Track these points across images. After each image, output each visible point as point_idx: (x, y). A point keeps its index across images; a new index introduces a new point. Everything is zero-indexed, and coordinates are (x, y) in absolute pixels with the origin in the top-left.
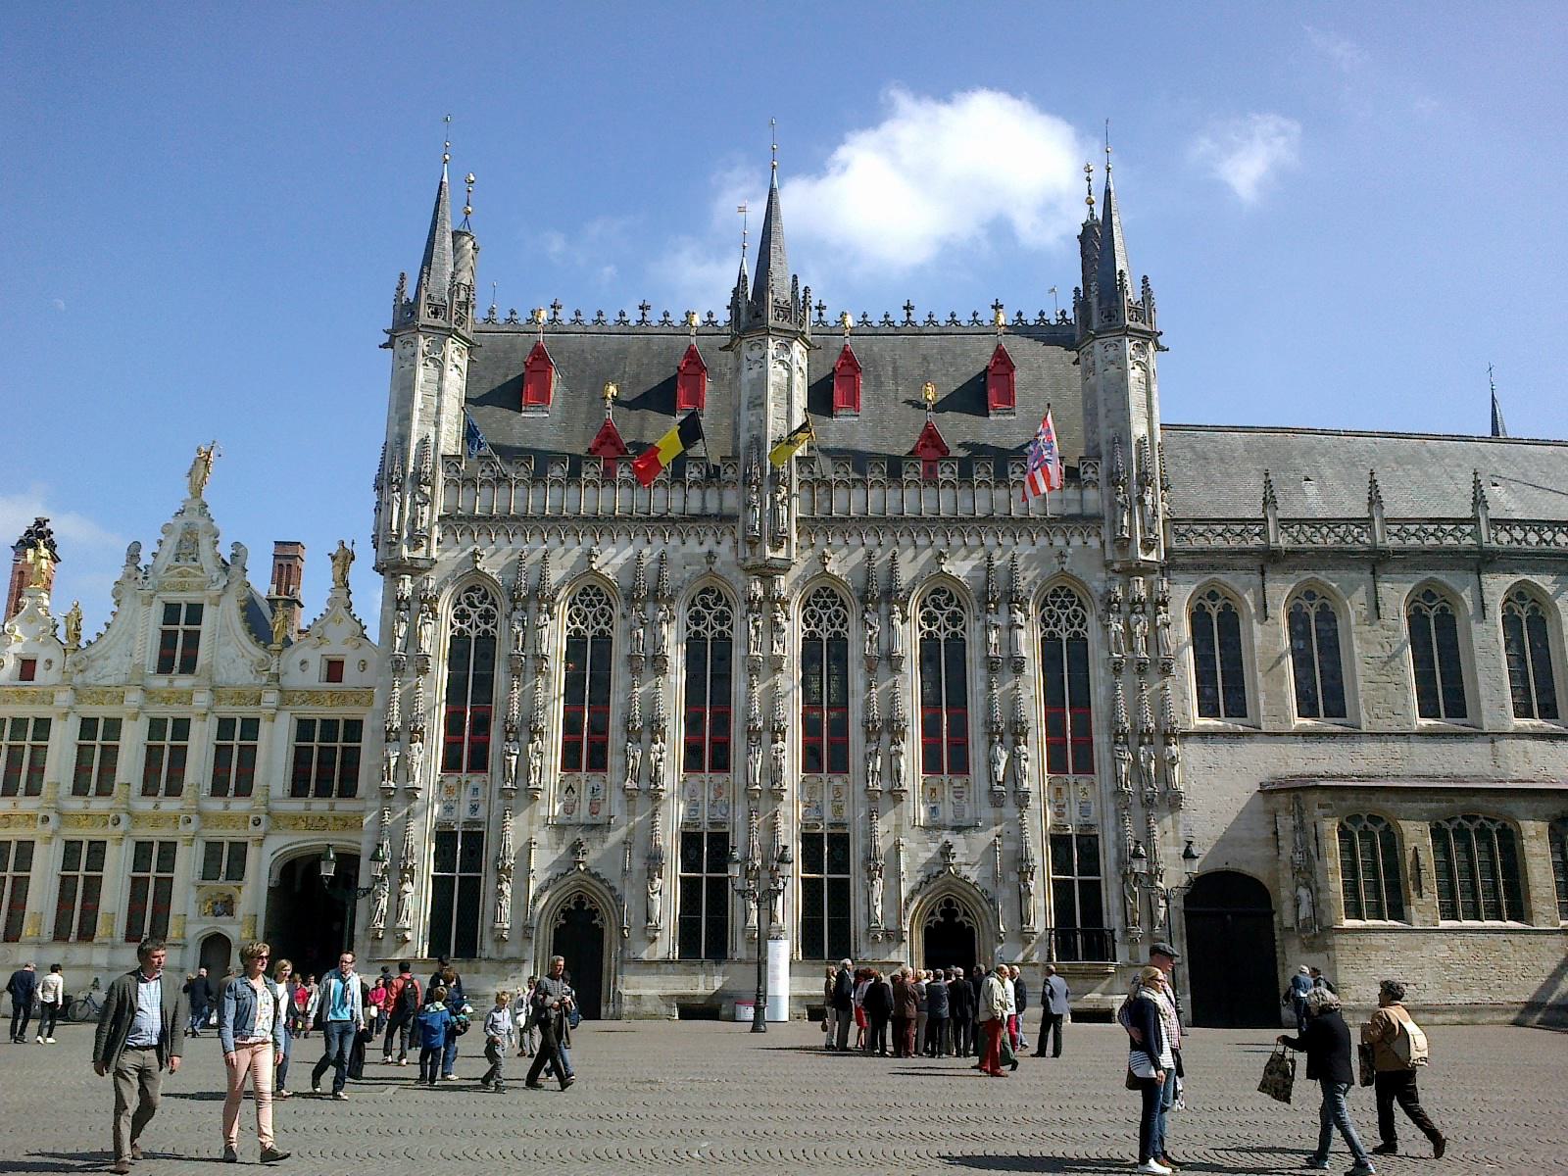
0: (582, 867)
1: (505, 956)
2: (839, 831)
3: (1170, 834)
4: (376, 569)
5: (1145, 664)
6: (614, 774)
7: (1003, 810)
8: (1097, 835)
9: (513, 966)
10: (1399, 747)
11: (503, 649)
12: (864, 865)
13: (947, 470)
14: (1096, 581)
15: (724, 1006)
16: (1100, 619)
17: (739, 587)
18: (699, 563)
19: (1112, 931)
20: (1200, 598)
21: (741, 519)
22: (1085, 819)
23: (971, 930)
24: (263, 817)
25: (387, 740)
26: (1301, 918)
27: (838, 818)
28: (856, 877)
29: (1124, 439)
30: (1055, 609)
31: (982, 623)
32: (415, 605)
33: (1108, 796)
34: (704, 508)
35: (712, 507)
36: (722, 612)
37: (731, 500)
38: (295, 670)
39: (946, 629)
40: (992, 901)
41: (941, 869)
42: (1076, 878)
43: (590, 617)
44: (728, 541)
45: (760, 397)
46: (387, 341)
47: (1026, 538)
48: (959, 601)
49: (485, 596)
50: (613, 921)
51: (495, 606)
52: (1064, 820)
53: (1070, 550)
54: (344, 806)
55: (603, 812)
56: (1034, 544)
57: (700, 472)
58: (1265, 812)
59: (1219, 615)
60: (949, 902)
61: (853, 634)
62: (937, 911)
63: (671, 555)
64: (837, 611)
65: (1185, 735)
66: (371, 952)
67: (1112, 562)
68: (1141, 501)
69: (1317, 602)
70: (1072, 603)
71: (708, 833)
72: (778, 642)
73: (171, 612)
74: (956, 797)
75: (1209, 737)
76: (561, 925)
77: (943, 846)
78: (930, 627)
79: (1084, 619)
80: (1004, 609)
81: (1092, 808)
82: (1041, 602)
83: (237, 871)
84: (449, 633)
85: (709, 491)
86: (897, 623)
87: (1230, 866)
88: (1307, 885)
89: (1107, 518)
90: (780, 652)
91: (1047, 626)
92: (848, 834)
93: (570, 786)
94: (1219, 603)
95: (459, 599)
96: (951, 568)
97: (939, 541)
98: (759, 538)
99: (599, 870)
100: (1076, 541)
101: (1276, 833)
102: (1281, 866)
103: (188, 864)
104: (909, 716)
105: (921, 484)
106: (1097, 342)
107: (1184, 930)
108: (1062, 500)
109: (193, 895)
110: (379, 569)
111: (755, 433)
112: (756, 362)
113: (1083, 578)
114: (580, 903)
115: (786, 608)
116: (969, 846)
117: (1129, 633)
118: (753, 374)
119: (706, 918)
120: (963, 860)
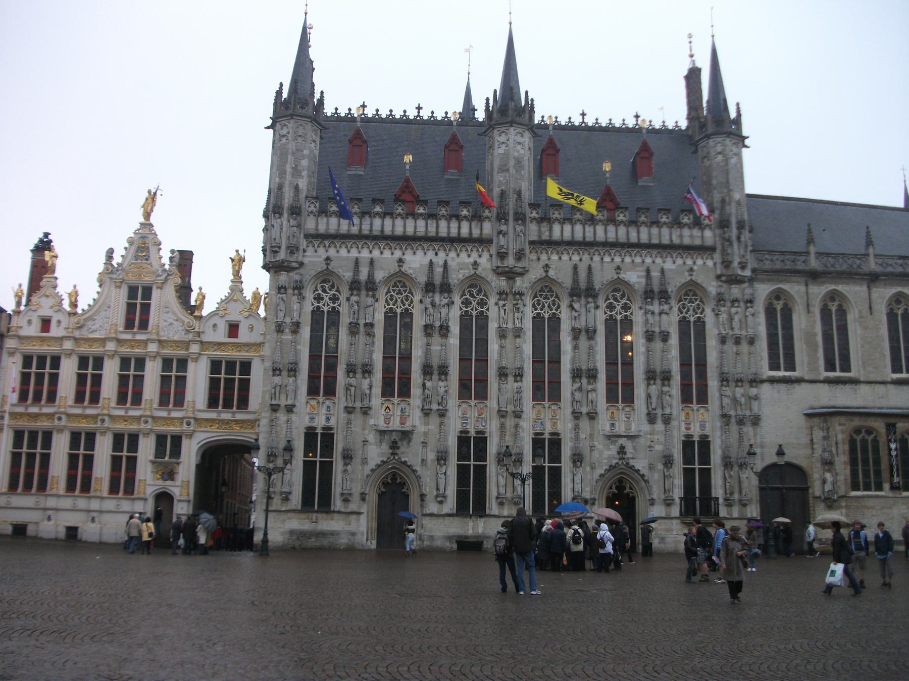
0: (397, 458)
1: (349, 510)
4: (264, 267)
7: (655, 426)
9: (354, 517)
10: (880, 389)
11: (345, 319)
13: (622, 215)
14: (713, 288)
15: (485, 542)
16: (713, 310)
17: (493, 284)
18: (468, 268)
19: (717, 499)
21: (494, 242)
23: (634, 498)
24: (192, 421)
25: (274, 375)
26: (826, 489)
30: (686, 303)
31: (643, 311)
32: (290, 291)
34: (471, 233)
35: (476, 233)
36: (482, 299)
37: (488, 228)
40: (646, 482)
41: (617, 461)
42: (697, 466)
43: (399, 300)
44: (486, 255)
45: (506, 165)
46: (270, 124)
47: (669, 260)
49: (333, 286)
50: (416, 492)
51: (340, 293)
52: (690, 432)
54: (240, 416)
56: (674, 263)
57: (468, 211)
58: (806, 428)
59: (782, 309)
61: (565, 315)
62: (614, 487)
63: (450, 263)
65: (762, 381)
68: (739, 238)
69: (836, 303)
71: (474, 437)
73: (133, 292)
74: (627, 418)
79: (703, 310)
80: (656, 302)
81: (707, 425)
82: (678, 299)
83: (176, 452)
84: (311, 308)
85: (474, 224)
86: (593, 310)
88: (829, 471)
90: (518, 325)
91: (682, 313)
92: (560, 440)
93: (388, 407)
94: (781, 302)
95: (316, 287)
97: (618, 259)
98: (507, 253)
99: (407, 459)
100: (700, 262)
101: (812, 440)
102: (814, 460)
103: (146, 449)
104: (599, 368)
105: (605, 222)
106: (711, 141)
109: (150, 467)
110: (266, 267)
111: (503, 188)
112: (503, 143)
113: (704, 285)
114: (394, 476)
116: (634, 448)
117: (731, 319)
118: (501, 151)
120: (631, 456)
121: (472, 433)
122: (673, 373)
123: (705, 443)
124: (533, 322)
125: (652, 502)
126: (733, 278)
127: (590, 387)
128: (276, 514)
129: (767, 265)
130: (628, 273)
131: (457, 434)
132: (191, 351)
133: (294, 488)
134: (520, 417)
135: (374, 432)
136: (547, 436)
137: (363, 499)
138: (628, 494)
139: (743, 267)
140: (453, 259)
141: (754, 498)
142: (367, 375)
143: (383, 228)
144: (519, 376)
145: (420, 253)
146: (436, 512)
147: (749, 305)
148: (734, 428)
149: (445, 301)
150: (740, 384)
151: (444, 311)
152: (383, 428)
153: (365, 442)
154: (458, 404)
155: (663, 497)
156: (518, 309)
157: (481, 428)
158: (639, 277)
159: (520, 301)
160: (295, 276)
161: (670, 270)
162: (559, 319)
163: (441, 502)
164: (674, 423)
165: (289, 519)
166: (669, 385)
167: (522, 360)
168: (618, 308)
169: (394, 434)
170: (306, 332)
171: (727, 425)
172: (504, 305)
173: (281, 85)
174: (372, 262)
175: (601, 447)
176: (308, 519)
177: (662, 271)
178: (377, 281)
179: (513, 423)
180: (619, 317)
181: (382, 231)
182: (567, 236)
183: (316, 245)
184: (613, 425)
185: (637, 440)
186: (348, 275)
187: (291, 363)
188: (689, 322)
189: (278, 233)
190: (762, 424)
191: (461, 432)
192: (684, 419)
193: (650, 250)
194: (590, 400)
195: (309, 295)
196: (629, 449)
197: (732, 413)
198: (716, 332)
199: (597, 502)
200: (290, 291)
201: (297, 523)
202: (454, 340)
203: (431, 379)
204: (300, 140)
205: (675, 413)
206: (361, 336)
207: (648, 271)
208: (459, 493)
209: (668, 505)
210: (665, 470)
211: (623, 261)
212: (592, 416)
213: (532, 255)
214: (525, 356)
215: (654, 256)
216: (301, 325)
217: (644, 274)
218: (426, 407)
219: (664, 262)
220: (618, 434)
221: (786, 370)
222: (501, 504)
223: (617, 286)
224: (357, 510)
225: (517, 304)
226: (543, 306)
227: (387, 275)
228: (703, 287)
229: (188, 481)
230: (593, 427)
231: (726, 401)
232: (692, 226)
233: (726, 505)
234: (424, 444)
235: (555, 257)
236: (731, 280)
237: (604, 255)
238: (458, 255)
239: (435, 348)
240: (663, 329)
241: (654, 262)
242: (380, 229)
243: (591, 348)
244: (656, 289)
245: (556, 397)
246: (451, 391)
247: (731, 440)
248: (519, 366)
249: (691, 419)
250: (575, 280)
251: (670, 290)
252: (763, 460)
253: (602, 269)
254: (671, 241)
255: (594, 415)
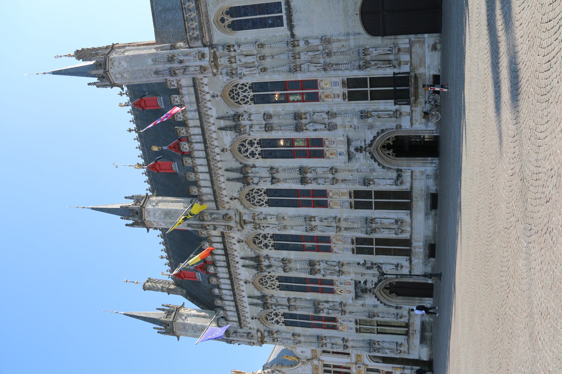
1: (408, 315)
2: (353, 195)
3: (344, 43)
5: (260, 57)
6: (335, 278)
7: (338, 124)
8: (348, 79)
11: (287, 311)
12: (367, 186)
14: (223, 79)
17: (252, 232)
19: (394, 74)
20: (224, 27)
22: (340, 84)
24: (357, 366)
27: (347, 194)
28: (373, 188)
29: (155, 70)
30: (240, 98)
31: (251, 133)
32: (275, 336)
33: (327, 74)
36: (262, 237)
38: (305, 355)
39: (256, 147)
40: (383, 131)
41: (368, 153)
42: (369, 89)
44: (232, 234)
48: (243, 141)
49: (269, 315)
52: (341, 95)
53: (211, 92)
55: (350, 281)
56: (211, 109)
57: (206, 243)
59: (232, 16)
60: (383, 147)
62: (387, 152)
64: (255, 193)
65: (293, 35)
66: (405, 353)
67: (213, 73)
68: (181, 62)
70: (236, 90)
71: (357, 245)
72: (271, 218)
75: (293, 23)
76: (396, 294)
77: (357, 152)
78: (256, 154)
79: (243, 84)
81: (334, 80)
82: (237, 105)
87: (358, 12)
89: (193, 76)
92: (354, 191)
93: (340, 292)
94: (226, 18)
96: (228, 146)
98: (228, 226)
100: (206, 89)
107: (393, 37)
108: (189, 96)
115: (256, 214)
116: (357, 140)
117: (247, 66)
118: (162, 224)
119: (393, 246)
120: (363, 143)
121: (354, 246)
122: (296, 110)
123: (350, 83)
124: (272, 206)
125: (399, 127)
126: (213, 63)
127: (313, 172)
128: (410, 349)
129: (197, 33)
130: (225, 143)
131: (355, 255)
132: (318, 364)
133: (394, 341)
134: (340, 219)
135: (357, 301)
136: (353, 200)
137: (401, 308)
138: (393, 142)
139: (203, 56)
140: (239, 253)
141: (393, 41)
142: (321, 304)
143: (227, 290)
144: (311, 218)
145: (238, 271)
146: (409, 269)
147: (232, 49)
148: (334, 59)
149: (267, 260)
150: (297, 56)
151: (273, 262)
152: (354, 294)
153: (363, 305)
154: (334, 254)
155: (394, 119)
156: (264, 218)
157: (350, 240)
158: (227, 135)
159: (259, 216)
160: (266, 334)
161: (217, 112)
162: (267, 190)
163: (402, 267)
164: (335, 109)
165: (413, 343)
166: (305, 114)
167: (299, 216)
168: (253, 149)
169: (357, 290)
170: (298, 330)
171: (332, 66)
172: (263, 227)
173: (158, 332)
174: (249, 297)
175: (358, 165)
176: (413, 335)
177: (219, 118)
178: (261, 294)
179: (345, 223)
180: (260, 149)
181: (230, 290)
182: (209, 184)
183: (246, 323)
184: (340, 154)
185: (350, 138)
186: (260, 309)
187: (318, 340)
188: (254, 95)
189: (242, 342)
190: (328, 34)
191: (353, 253)
192: (330, 99)
193: (205, 127)
194: (322, 173)
195: (275, 327)
196: (358, 144)
197: (322, 61)
198: (258, 75)
199: (400, 168)
200: (275, 336)
201: (416, 339)
202: (292, 255)
203: (319, 270)
204: (186, 327)
205: (326, 109)
206: (297, 304)
207: (221, 129)
208: (395, 255)
209: (401, 113)
210: (373, 117)
211: (217, 147)
212: (333, 170)
213: (226, 207)
214: (297, 214)
215: (209, 124)
216: (295, 332)
217: (223, 132)
218: (338, 275)
219: (212, 116)
220: (347, 151)
221: (281, 12)
222: (402, 231)
223: (237, 150)
224: (408, 311)
225: (261, 220)
226: (260, 199)
227: (256, 290)
228: (225, 87)
229: (393, 367)
230: (344, 170)
231: (312, 68)
232: (181, 96)
233: (399, 64)
234: (363, 274)
235: (224, 192)
236: (215, 65)
237: (216, 160)
238: (236, 250)
239: (298, 266)
240: (262, 119)
241: (214, 124)
242: (229, 291)
243: (284, 170)
244: (234, 123)
245: (324, 193)
246: (326, 259)
247: (345, 62)
248: (304, 220)
249: (331, 94)
250: (238, 180)
251: (233, 113)
252: (359, 34)
253: (226, 161)
254: (195, 111)
255: (334, 170)
